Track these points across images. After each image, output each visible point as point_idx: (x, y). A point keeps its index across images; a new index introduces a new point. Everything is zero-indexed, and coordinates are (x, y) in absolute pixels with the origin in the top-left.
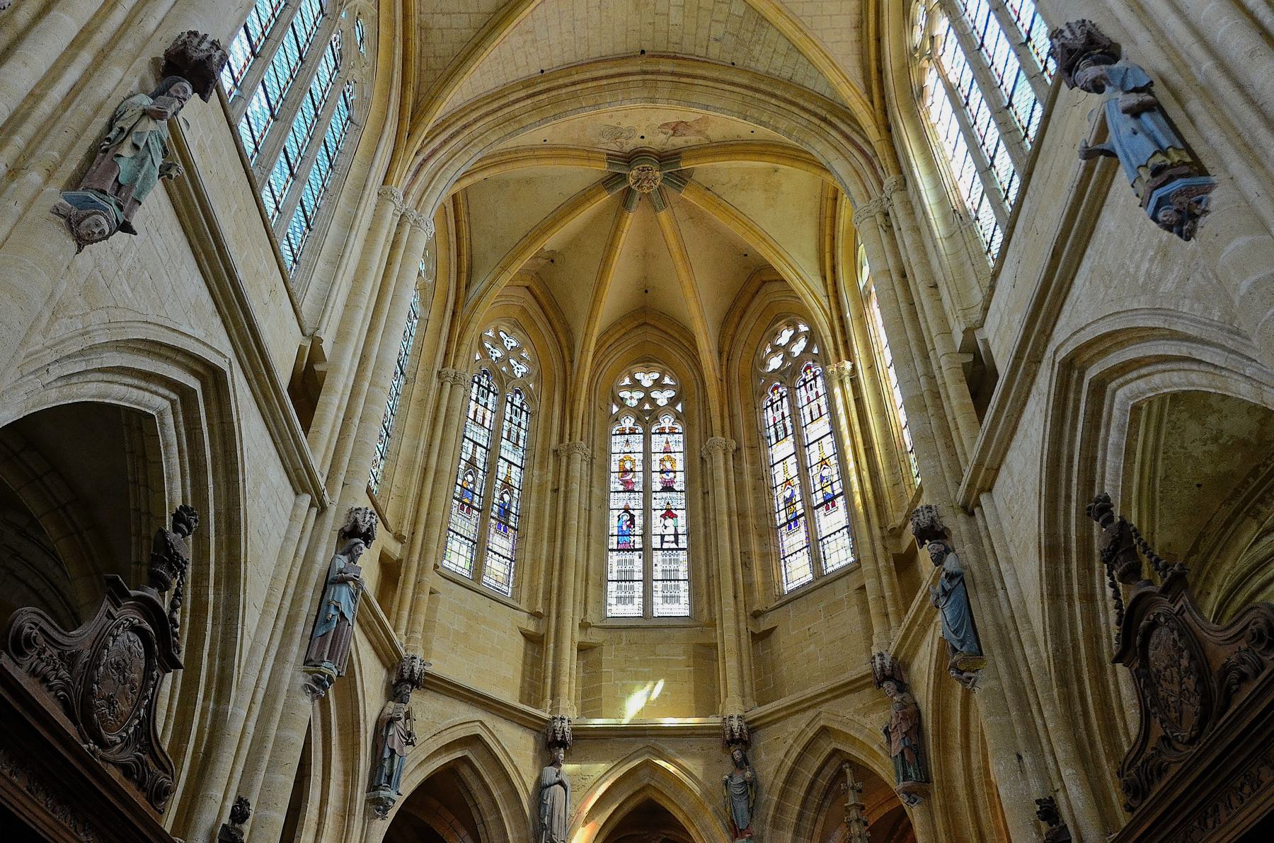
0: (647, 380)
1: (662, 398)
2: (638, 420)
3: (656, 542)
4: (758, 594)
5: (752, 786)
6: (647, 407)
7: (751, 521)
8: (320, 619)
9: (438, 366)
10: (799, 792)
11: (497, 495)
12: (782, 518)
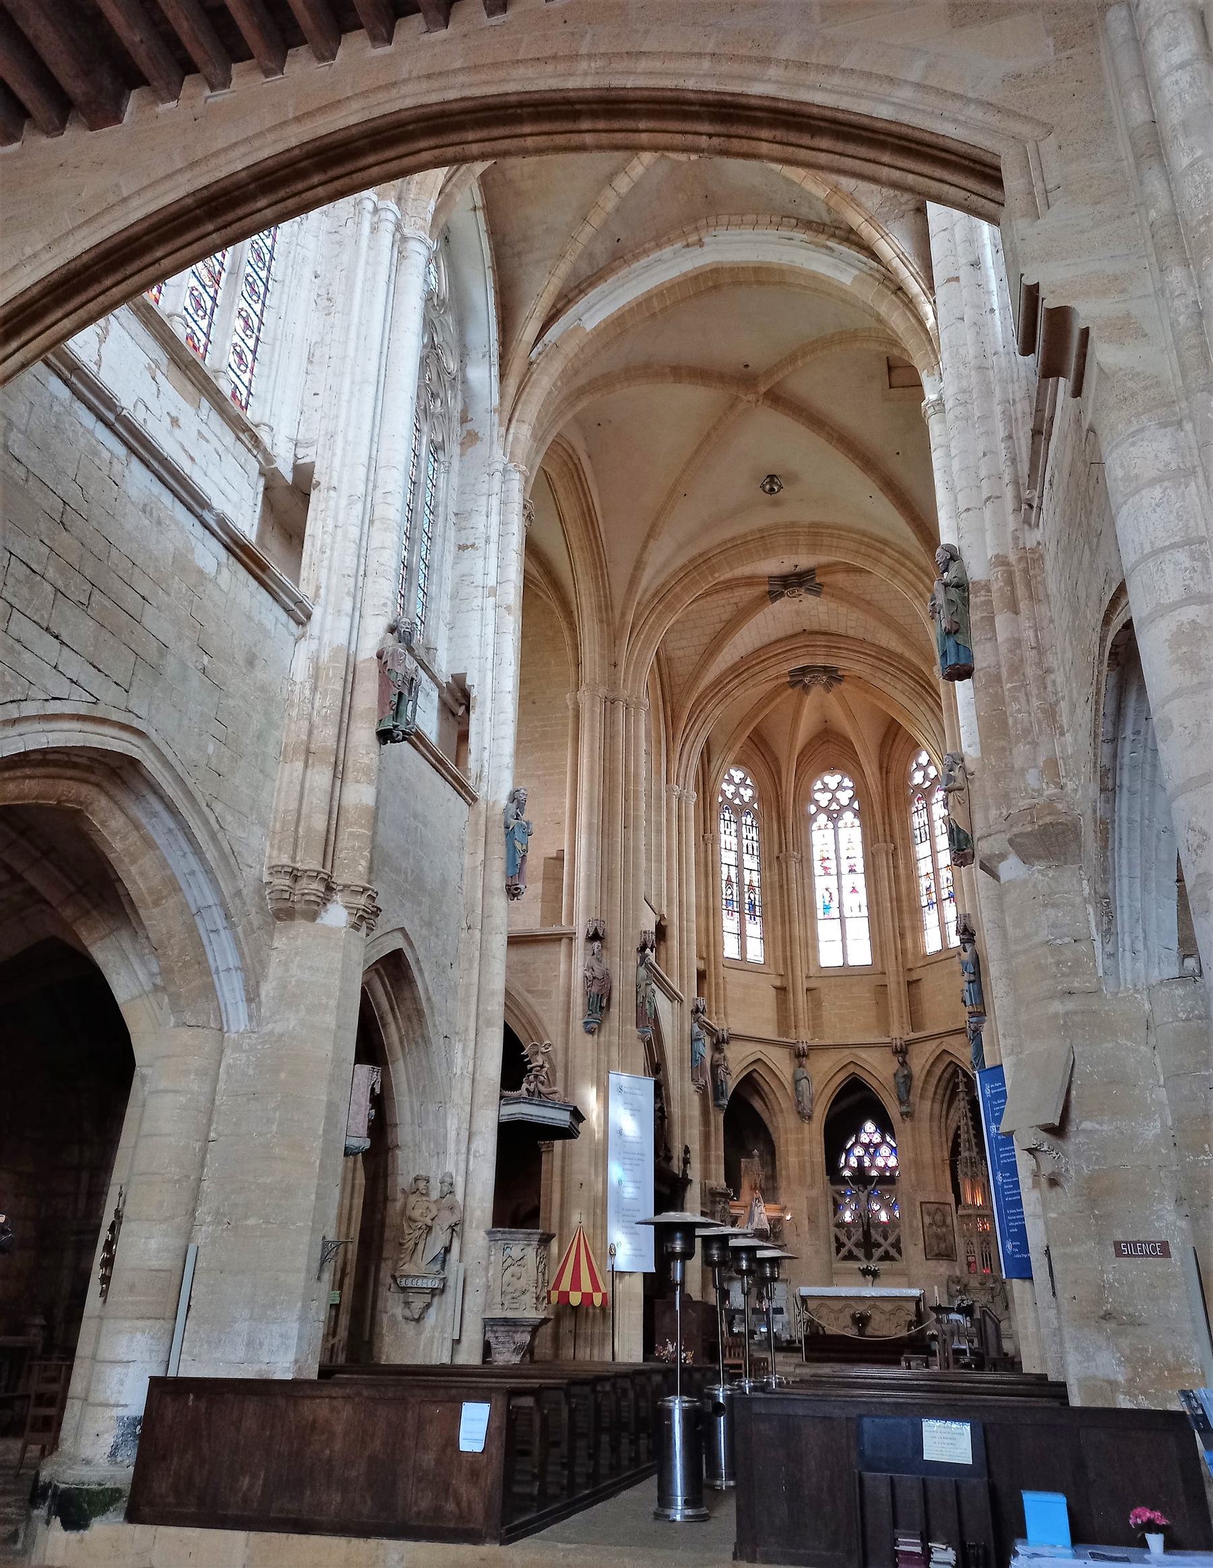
0: (832, 780)
1: (844, 797)
2: (830, 818)
3: (847, 913)
4: (910, 957)
5: (909, 1078)
6: (834, 806)
7: (905, 904)
8: (693, 1060)
9: (702, 833)
10: (934, 1081)
11: (746, 896)
12: (924, 903)
